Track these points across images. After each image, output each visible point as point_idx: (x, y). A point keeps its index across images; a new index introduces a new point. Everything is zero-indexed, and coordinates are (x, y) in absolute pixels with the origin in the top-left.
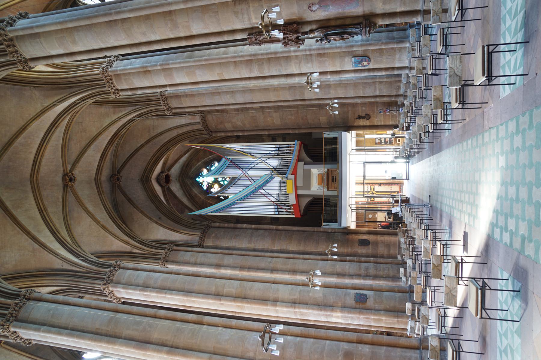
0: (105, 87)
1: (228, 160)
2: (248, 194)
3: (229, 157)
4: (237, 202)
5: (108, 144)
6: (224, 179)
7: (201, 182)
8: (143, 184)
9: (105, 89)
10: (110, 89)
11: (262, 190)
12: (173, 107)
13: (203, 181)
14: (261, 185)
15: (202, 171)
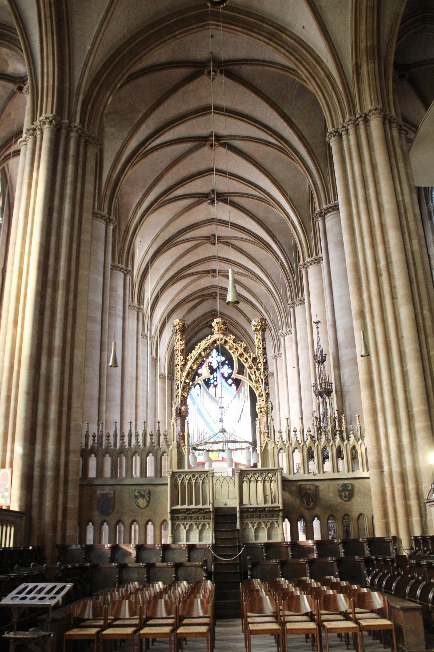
0: (286, 328)
1: (235, 397)
2: (203, 416)
3: (237, 396)
4: (196, 406)
5: (246, 298)
6: (215, 379)
7: (212, 355)
8: (209, 312)
9: (285, 328)
10: (285, 331)
11: (207, 429)
12: (278, 360)
13: (213, 357)
14: (212, 429)
15: (223, 356)
